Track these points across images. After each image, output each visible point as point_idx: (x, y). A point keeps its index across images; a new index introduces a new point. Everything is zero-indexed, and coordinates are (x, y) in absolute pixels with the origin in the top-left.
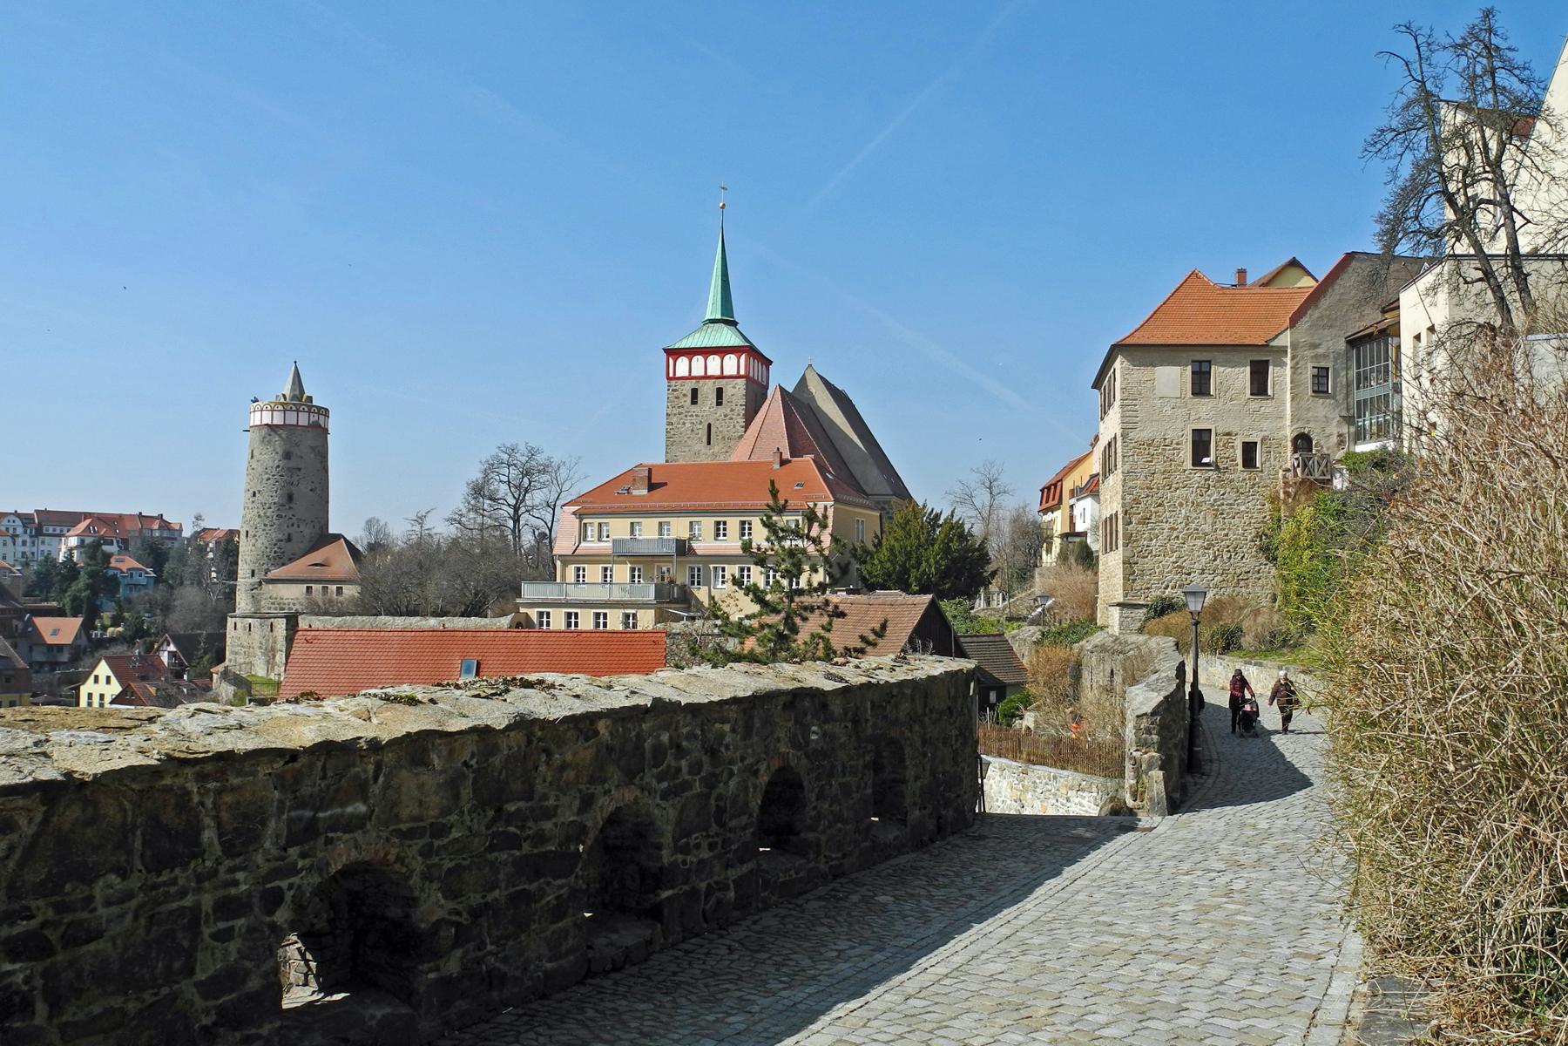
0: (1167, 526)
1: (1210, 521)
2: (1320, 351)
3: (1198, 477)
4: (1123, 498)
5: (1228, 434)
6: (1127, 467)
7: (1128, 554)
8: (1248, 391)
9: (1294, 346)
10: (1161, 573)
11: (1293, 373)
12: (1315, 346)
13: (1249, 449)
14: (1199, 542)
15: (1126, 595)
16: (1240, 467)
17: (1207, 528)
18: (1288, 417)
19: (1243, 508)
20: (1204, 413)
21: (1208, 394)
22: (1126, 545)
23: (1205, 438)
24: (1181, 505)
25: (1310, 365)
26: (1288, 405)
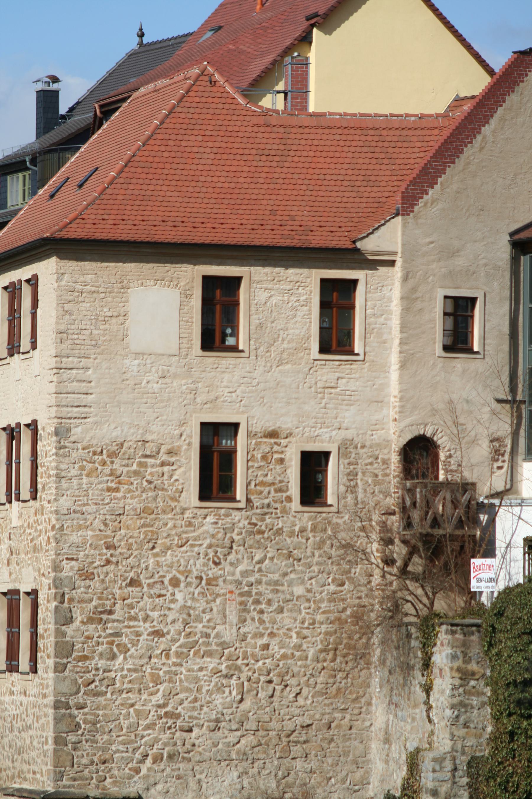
0: (145, 628)
1: (233, 617)
2: (460, 262)
3: (212, 519)
4: (56, 568)
5: (273, 434)
6: (65, 502)
7: (65, 687)
8: (315, 346)
9: (411, 251)
10: (133, 728)
11: (406, 310)
12: (452, 253)
13: (313, 464)
14: (211, 663)
15: (59, 776)
16: (296, 504)
17: (228, 634)
18: (394, 401)
19: (299, 590)
20: (228, 388)
21: (235, 349)
22: (60, 668)
23: (226, 443)
24: (175, 583)
25: (440, 293)
26: (394, 376)
